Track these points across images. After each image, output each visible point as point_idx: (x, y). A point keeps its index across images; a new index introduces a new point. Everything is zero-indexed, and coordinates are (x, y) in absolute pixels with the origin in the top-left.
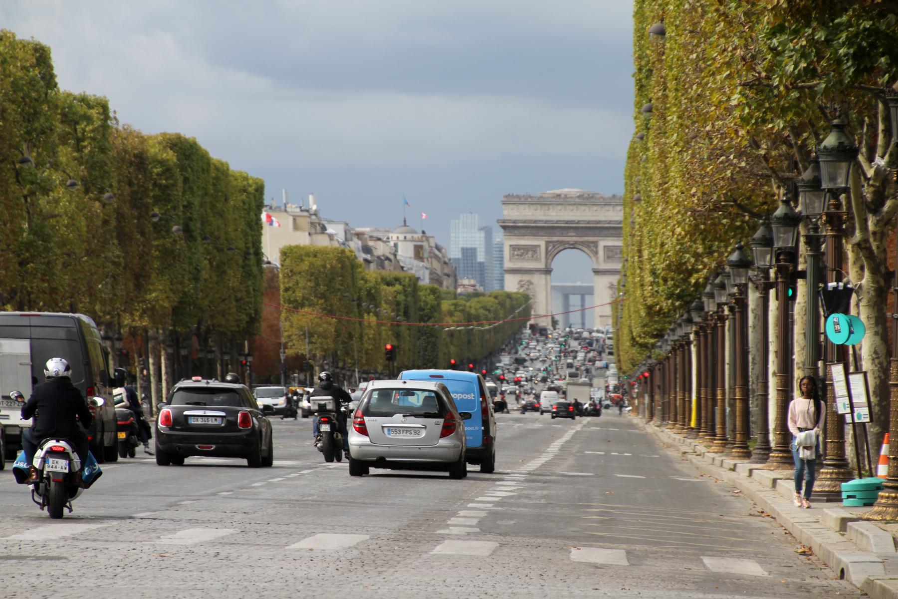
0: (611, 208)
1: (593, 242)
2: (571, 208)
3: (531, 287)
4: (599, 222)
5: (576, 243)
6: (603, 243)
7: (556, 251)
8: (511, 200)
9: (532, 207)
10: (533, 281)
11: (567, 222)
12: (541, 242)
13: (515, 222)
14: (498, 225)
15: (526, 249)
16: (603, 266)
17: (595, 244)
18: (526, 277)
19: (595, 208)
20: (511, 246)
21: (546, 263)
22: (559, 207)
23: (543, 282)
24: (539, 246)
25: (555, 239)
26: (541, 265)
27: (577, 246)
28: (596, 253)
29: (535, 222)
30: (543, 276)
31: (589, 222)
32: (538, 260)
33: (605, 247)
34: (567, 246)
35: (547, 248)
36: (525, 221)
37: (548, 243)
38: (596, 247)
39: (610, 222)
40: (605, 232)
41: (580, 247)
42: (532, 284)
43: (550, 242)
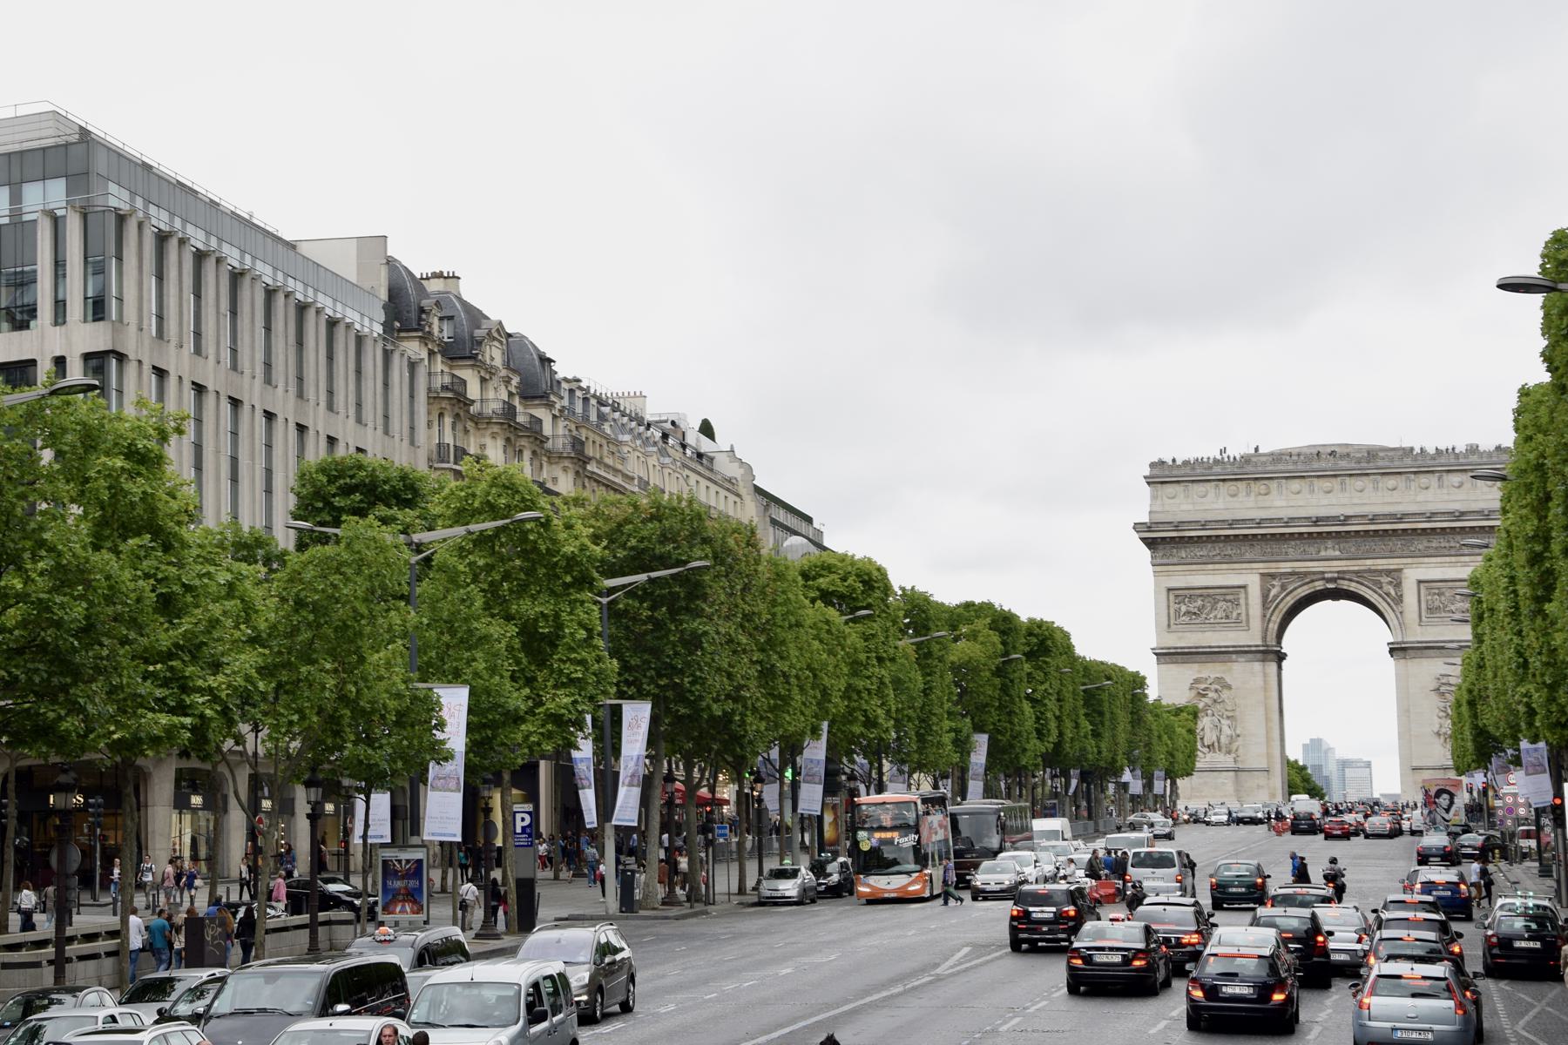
0: (1433, 479)
1: (1388, 572)
2: (1326, 484)
3: (1225, 694)
4: (1401, 518)
5: (1342, 575)
6: (1415, 572)
7: (1290, 601)
8: (1163, 476)
9: (1224, 487)
10: (1228, 680)
11: (1317, 521)
12: (1250, 578)
13: (1177, 526)
14: (1135, 537)
15: (1210, 595)
16: (1417, 634)
17: (1395, 576)
18: (1210, 671)
19: (1391, 482)
20: (1169, 590)
21: (1265, 631)
22: (1295, 485)
23: (1259, 681)
24: (1244, 587)
25: (1286, 567)
26: (1252, 637)
27: (1345, 585)
28: (1399, 599)
29: (1232, 524)
30: (1257, 666)
31: (1374, 519)
32: (1241, 623)
33: (1420, 582)
34: (1319, 585)
35: (1265, 596)
36: (1204, 525)
37: (1267, 577)
38: (1398, 585)
39: (1432, 516)
40: (1421, 544)
41: (1353, 587)
42: (1229, 687)
43: (1273, 576)
